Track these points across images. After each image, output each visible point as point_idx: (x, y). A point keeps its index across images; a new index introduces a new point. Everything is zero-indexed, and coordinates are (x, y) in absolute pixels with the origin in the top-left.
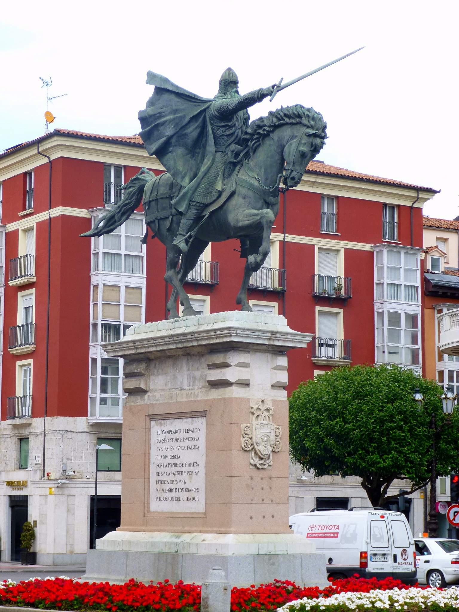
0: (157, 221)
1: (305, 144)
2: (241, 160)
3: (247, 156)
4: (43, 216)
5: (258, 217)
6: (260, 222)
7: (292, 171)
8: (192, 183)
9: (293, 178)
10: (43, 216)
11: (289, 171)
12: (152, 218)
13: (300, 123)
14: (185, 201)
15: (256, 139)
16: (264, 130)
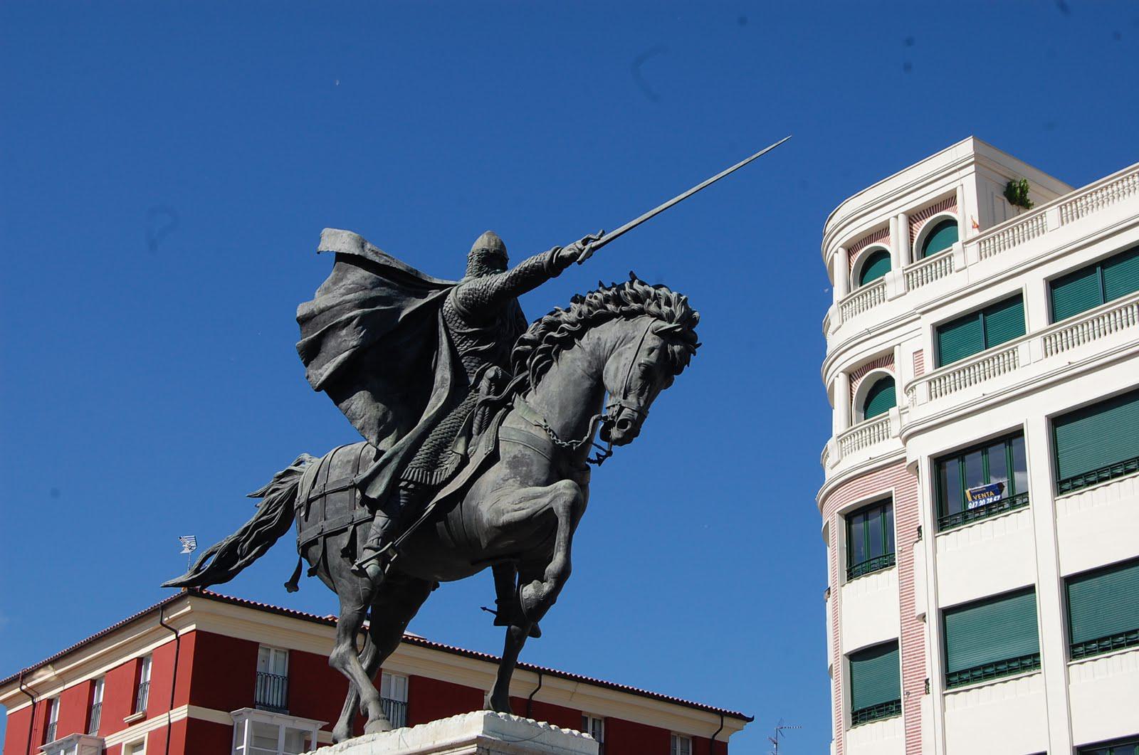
0: (321, 540)
1: (651, 350)
2: (509, 398)
3: (522, 388)
4: (159, 722)
5: (546, 500)
6: (551, 509)
7: (622, 408)
8: (401, 442)
9: (623, 424)
10: (159, 722)
11: (617, 408)
12: (310, 533)
13: (642, 312)
14: (384, 477)
15: (541, 351)
16: (563, 330)
